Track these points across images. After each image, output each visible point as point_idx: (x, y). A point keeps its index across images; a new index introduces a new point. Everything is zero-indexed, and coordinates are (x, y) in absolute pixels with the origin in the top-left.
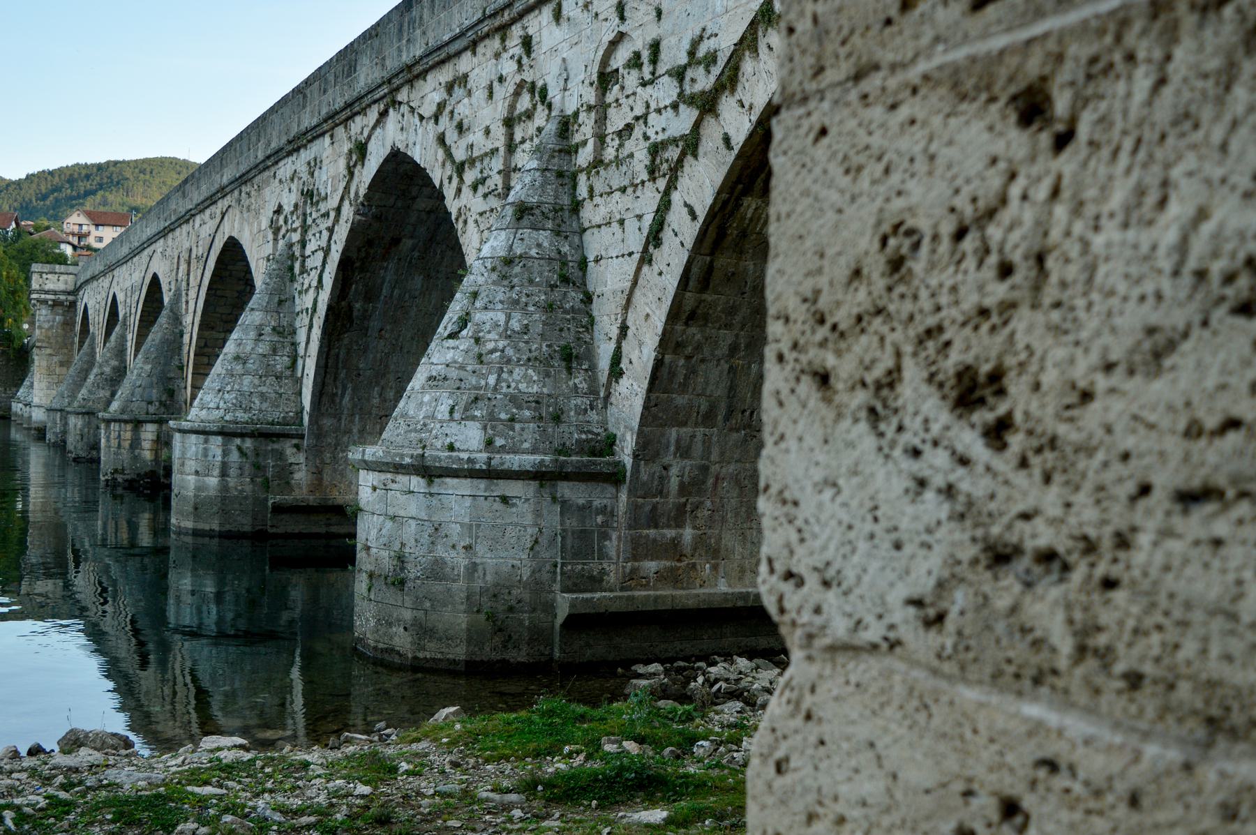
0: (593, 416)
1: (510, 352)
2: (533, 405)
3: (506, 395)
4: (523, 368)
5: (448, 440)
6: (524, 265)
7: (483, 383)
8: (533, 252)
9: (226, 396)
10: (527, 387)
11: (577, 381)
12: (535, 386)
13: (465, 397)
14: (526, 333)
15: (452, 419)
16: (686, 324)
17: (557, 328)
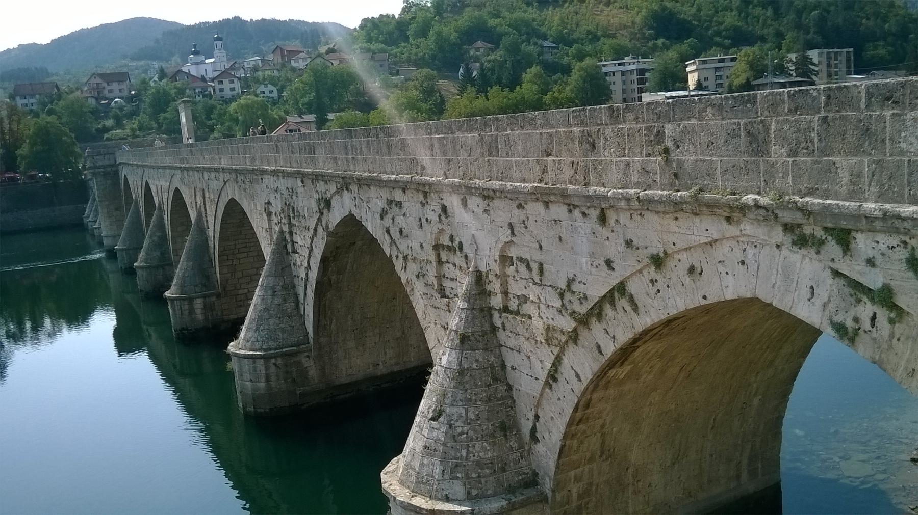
0: (523, 462)
1: (471, 433)
2: (490, 465)
3: (473, 462)
4: (480, 442)
5: (445, 493)
6: (471, 375)
7: (459, 455)
8: (474, 366)
9: (261, 332)
10: (485, 455)
11: (511, 444)
12: (489, 454)
13: (450, 465)
14: (478, 420)
15: (444, 480)
16: (578, 425)
17: (495, 412)
